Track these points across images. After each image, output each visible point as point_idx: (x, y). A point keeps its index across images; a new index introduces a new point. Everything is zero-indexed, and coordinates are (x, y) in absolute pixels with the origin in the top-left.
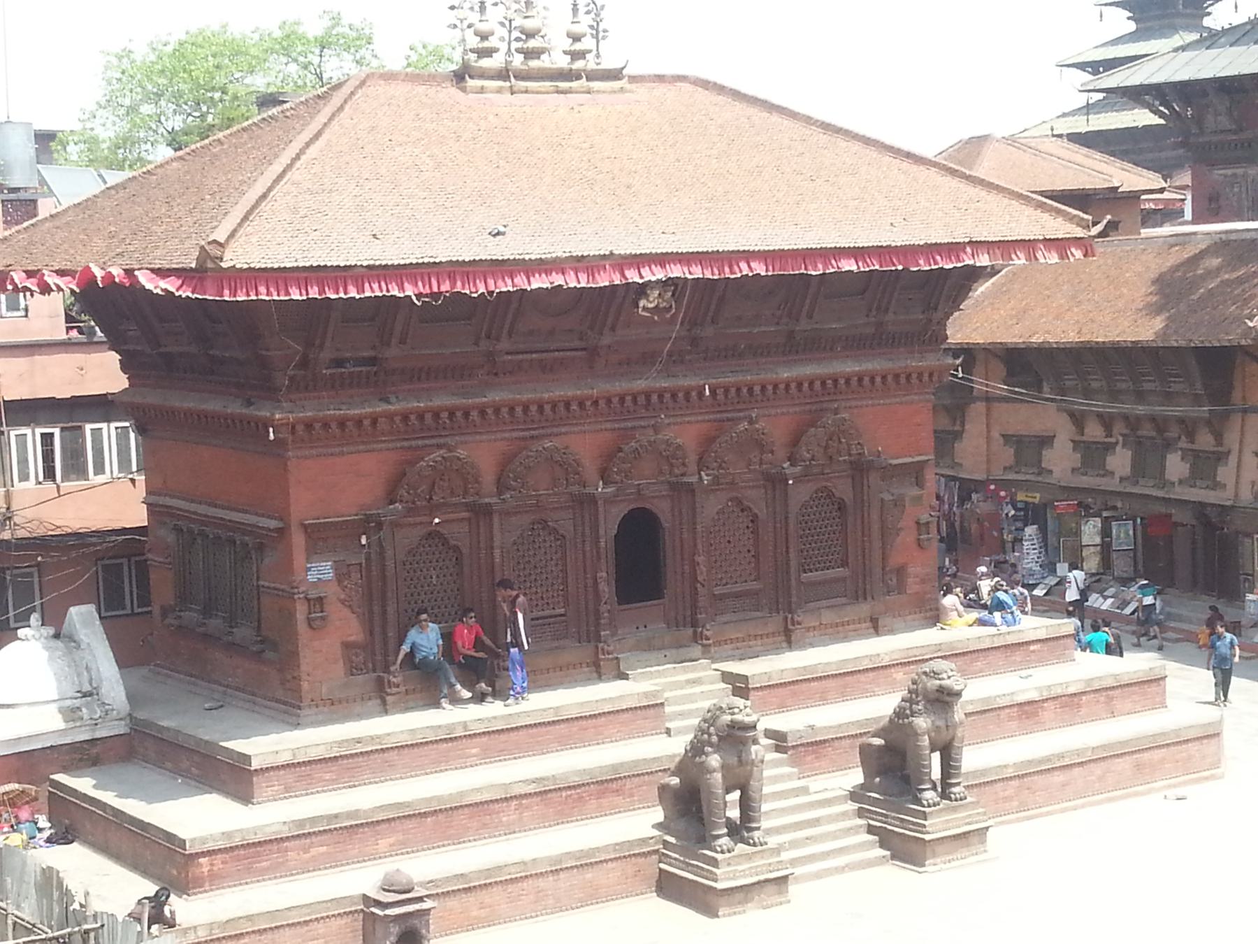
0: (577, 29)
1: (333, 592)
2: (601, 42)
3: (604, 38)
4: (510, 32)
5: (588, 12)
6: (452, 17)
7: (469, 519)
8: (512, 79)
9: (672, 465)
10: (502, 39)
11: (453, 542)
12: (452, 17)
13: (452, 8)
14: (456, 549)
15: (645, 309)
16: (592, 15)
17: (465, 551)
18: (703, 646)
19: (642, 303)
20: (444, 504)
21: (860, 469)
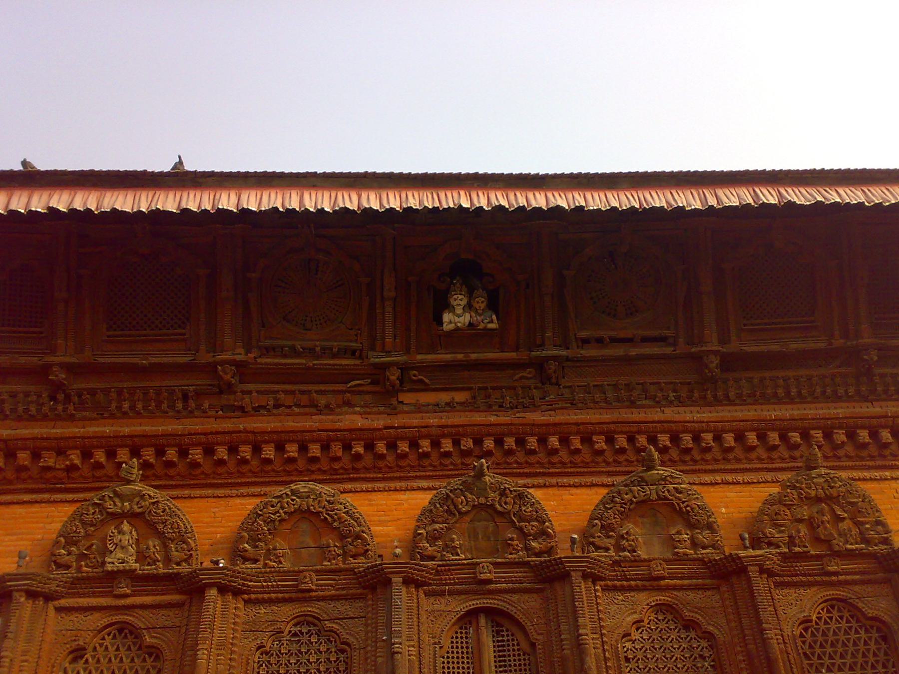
17: (167, 654)
19: (447, 317)
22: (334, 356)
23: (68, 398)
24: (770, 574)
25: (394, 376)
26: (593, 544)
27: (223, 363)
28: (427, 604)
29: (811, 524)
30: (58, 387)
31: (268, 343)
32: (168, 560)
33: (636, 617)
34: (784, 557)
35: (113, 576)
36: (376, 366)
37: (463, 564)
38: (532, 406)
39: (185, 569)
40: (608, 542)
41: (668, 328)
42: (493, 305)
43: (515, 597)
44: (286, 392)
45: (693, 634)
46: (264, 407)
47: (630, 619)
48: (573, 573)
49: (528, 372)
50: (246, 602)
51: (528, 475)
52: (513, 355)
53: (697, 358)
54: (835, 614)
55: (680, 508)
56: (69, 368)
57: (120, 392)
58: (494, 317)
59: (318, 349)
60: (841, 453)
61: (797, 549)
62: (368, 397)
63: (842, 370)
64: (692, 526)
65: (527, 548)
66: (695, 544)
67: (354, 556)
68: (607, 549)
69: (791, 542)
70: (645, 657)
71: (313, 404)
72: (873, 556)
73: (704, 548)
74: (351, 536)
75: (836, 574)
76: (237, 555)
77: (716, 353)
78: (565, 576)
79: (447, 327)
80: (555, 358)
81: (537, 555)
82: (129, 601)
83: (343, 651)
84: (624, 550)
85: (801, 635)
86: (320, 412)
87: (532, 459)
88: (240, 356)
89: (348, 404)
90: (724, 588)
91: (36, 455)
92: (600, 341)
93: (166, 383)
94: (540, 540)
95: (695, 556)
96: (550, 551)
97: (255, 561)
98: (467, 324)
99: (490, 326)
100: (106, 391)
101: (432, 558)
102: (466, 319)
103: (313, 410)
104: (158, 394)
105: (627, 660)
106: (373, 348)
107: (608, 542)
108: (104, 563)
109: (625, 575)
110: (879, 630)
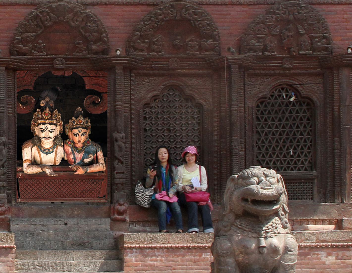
18: (114, 220)
26: (133, 47)
29: (280, 37)
33: (155, 93)
34: (258, 58)
37: (45, 58)
45: (189, 104)
47: (151, 95)
48: (116, 67)
55: (195, 25)
61: (267, 53)
65: (88, 49)
68: (142, 50)
69: (265, 49)
70: (157, 117)
75: (289, 69)
78: (112, 69)
84: (153, 51)
85: (258, 106)
94: (98, 44)
95: (200, 56)
96: (105, 52)
105: (145, 118)
109: (152, 67)
110: (308, 104)
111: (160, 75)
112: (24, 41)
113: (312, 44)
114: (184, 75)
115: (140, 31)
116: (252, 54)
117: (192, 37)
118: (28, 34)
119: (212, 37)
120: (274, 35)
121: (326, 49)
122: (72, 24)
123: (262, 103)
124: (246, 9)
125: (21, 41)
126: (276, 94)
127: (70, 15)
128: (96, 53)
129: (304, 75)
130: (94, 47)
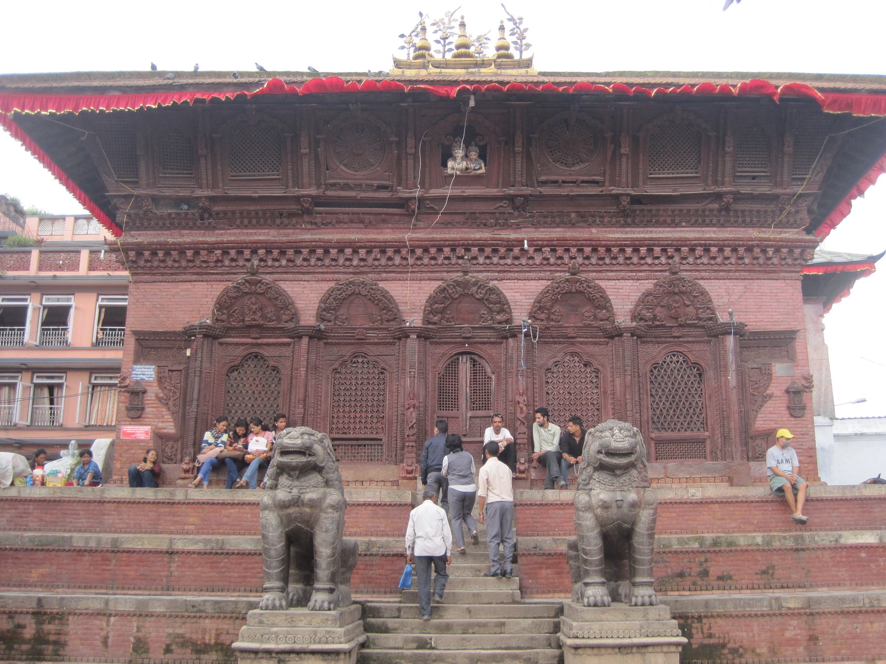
0: (501, 42)
1: (153, 391)
2: (524, 52)
3: (526, 49)
4: (444, 46)
5: (512, 34)
6: (402, 42)
7: (288, 344)
8: (430, 66)
9: (491, 310)
10: (438, 52)
11: (272, 363)
12: (402, 42)
13: (402, 36)
14: (274, 369)
15: (453, 169)
16: (517, 35)
17: (285, 372)
19: (450, 164)
20: (259, 326)
21: (716, 332)
22: (375, 191)
23: (211, 215)
24: (639, 337)
25: (415, 206)
27: (304, 196)
28: (430, 348)
30: (205, 210)
31: (331, 181)
32: (279, 320)
33: (555, 360)
34: (650, 327)
35: (249, 327)
36: (402, 199)
38: (506, 226)
39: (291, 325)
40: (543, 316)
41: (600, 175)
42: (482, 156)
43: (484, 347)
44: (344, 213)
46: (330, 223)
49: (504, 203)
50: (325, 343)
51: (499, 272)
52: (495, 190)
53: (617, 197)
54: (675, 359)
56: (212, 199)
57: (241, 213)
58: (483, 165)
59: (364, 186)
60: (699, 261)
61: (658, 323)
62: (397, 218)
63: (711, 206)
64: (597, 308)
65: (492, 319)
66: (595, 318)
67: (388, 321)
69: (655, 318)
71: (362, 222)
72: (703, 327)
73: (601, 320)
74: (387, 307)
75: (679, 337)
76: (321, 318)
77: (627, 195)
79: (449, 171)
80: (521, 196)
81: (500, 323)
82: (260, 341)
83: (382, 373)
84: (553, 320)
85: (652, 371)
86: (366, 227)
87: (502, 262)
88: (313, 191)
89: (384, 221)
90: (610, 345)
91: (197, 253)
92: (556, 182)
93: (270, 207)
96: (508, 321)
97: (330, 321)
98: (464, 167)
99: (479, 172)
100: (233, 213)
101: (435, 324)
102: (464, 164)
103: (361, 225)
104: (265, 214)
105: (547, 382)
106: (399, 184)
107: (543, 316)
108: (243, 320)
111: (560, 343)
112: (433, 312)
113: (697, 314)
114: (581, 343)
115: (539, 302)
116: (642, 323)
117: (587, 308)
118: (436, 306)
119: (605, 308)
120: (663, 306)
121: (711, 319)
122: (478, 296)
123: (655, 368)
124: (637, 283)
125: (431, 312)
126: (668, 360)
127: (475, 289)
128: (500, 323)
129: (693, 342)
130: (498, 317)
